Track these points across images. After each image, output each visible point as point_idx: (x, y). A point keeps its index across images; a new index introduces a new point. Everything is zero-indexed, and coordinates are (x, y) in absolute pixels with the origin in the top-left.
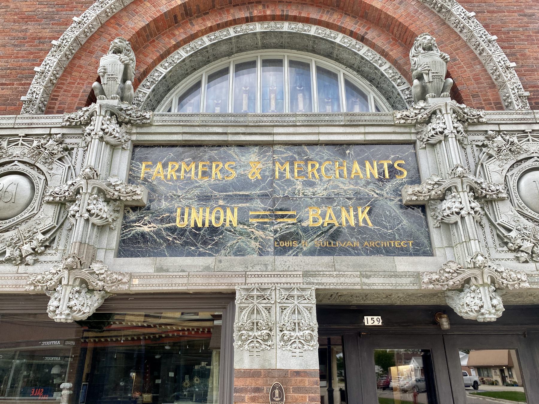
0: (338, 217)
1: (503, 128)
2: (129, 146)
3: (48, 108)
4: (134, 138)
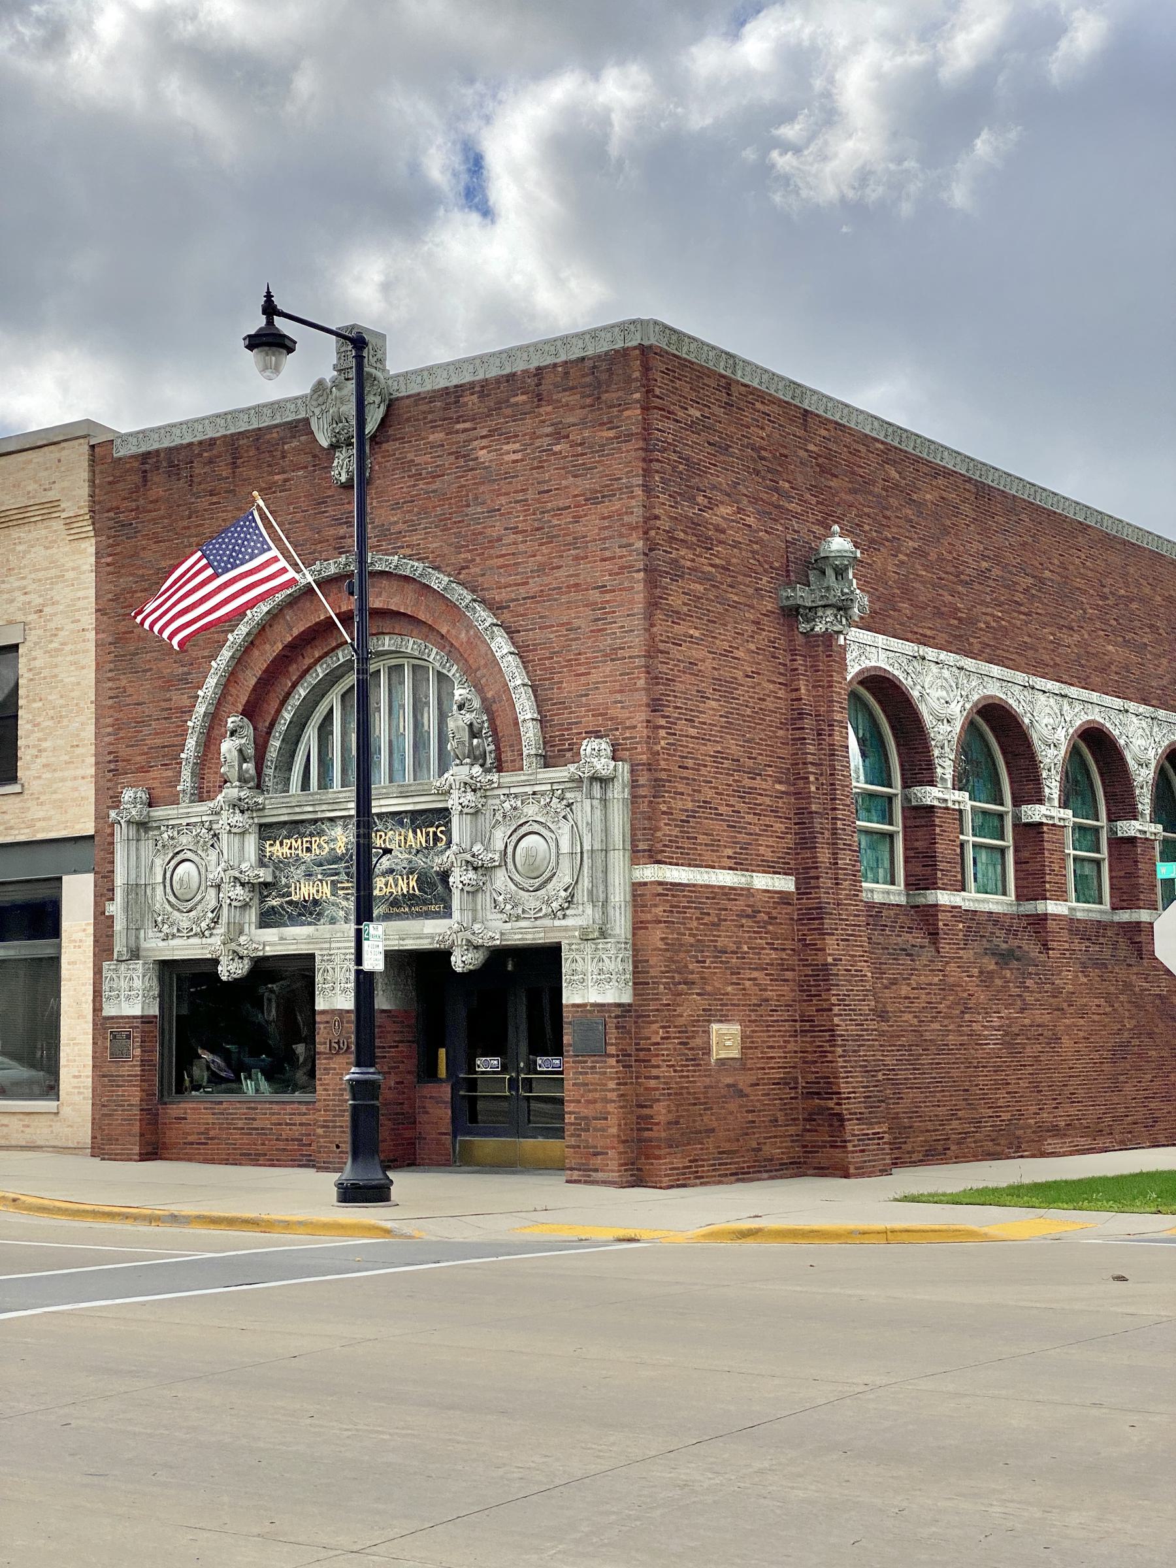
0: (396, 885)
1: (513, 790)
2: (255, 829)
4: (256, 821)
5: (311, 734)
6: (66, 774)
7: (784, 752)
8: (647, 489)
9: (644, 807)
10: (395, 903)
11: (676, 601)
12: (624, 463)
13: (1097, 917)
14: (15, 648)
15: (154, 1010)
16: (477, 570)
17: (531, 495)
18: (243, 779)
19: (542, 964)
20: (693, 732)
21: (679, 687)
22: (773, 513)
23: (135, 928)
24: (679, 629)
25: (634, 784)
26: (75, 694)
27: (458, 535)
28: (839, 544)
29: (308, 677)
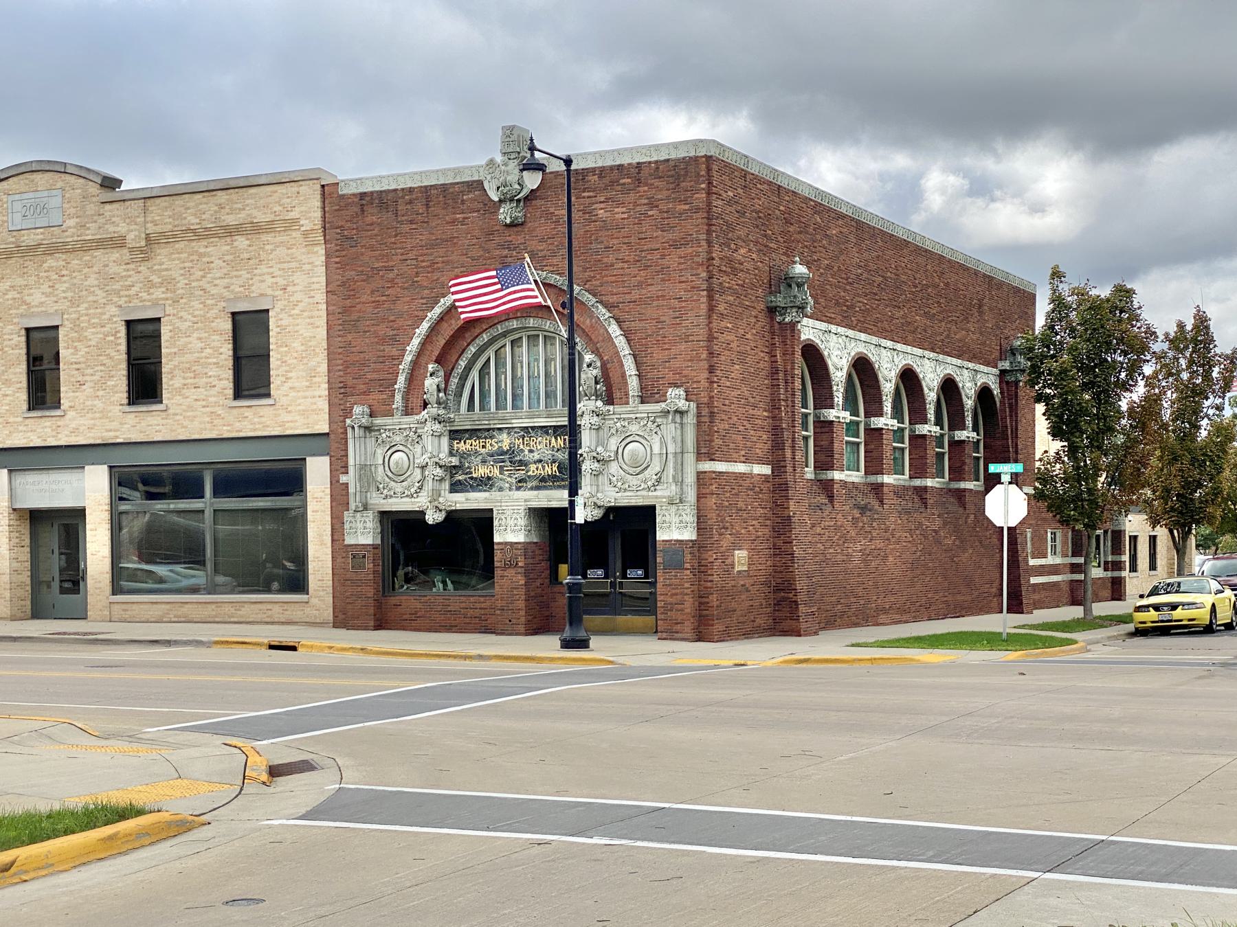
3: (407, 412)
5: (475, 375)
6: (307, 394)
7: (767, 393)
8: (709, 242)
9: (705, 428)
10: (543, 480)
11: (721, 308)
12: (694, 226)
13: (902, 483)
14: (267, 311)
15: (379, 542)
16: (598, 283)
17: (632, 240)
18: (439, 403)
19: (646, 515)
20: (728, 384)
21: (723, 358)
22: (764, 250)
23: (364, 491)
24: (723, 324)
25: (699, 415)
26: (313, 343)
27: (585, 261)
28: (800, 269)
29: (477, 341)
